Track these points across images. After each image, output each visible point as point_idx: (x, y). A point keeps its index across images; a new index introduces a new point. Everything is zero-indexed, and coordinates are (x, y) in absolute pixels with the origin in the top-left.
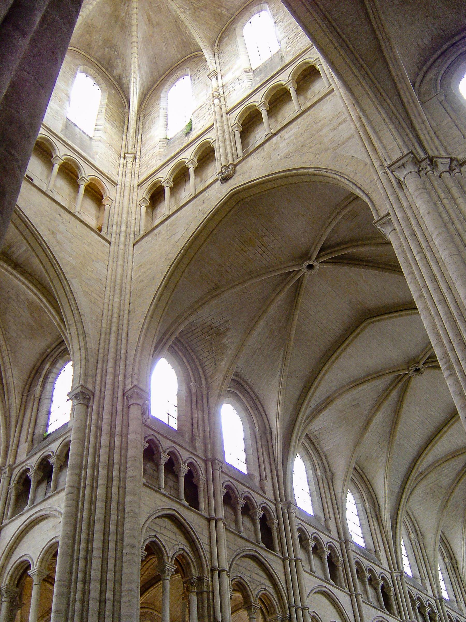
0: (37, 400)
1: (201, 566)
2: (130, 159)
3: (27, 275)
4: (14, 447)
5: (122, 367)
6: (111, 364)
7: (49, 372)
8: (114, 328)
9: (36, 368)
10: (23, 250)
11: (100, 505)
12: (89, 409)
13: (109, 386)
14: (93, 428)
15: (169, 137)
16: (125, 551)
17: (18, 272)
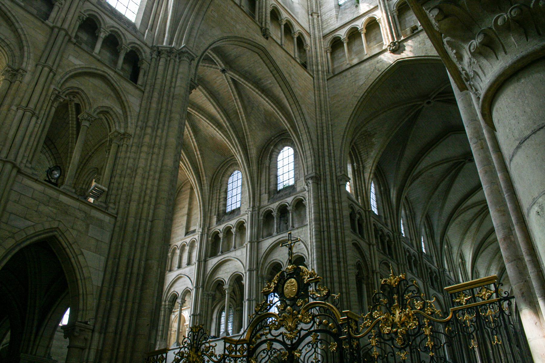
0: (268, 168)
1: (367, 270)
2: (315, 16)
3: (270, 97)
4: (258, 195)
5: (333, 161)
6: (327, 159)
7: (273, 151)
8: (325, 136)
9: (265, 148)
10: (268, 82)
11: (333, 242)
12: (319, 186)
13: (328, 173)
14: (323, 198)
15: (340, 3)
16: (348, 268)
17: (264, 95)
